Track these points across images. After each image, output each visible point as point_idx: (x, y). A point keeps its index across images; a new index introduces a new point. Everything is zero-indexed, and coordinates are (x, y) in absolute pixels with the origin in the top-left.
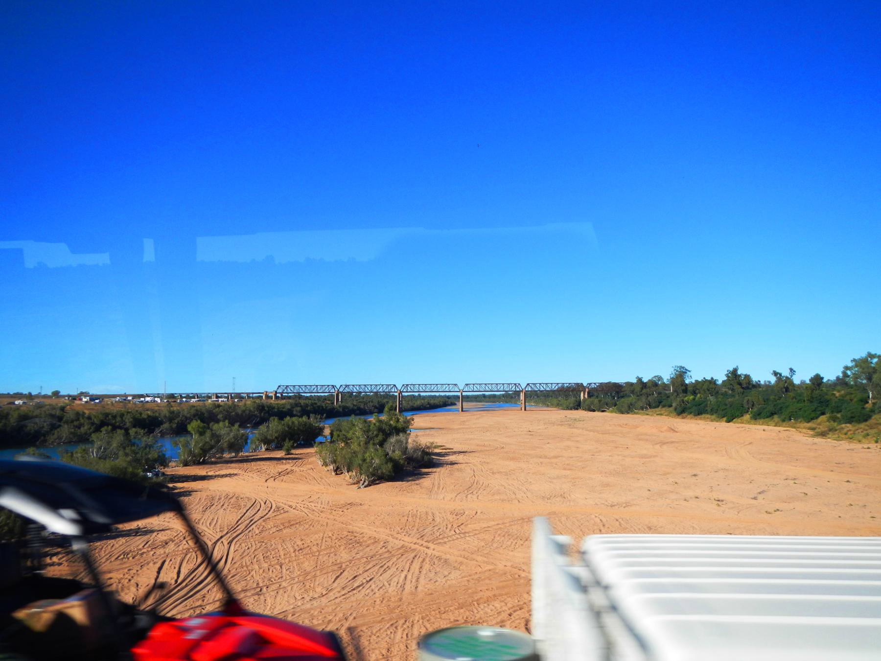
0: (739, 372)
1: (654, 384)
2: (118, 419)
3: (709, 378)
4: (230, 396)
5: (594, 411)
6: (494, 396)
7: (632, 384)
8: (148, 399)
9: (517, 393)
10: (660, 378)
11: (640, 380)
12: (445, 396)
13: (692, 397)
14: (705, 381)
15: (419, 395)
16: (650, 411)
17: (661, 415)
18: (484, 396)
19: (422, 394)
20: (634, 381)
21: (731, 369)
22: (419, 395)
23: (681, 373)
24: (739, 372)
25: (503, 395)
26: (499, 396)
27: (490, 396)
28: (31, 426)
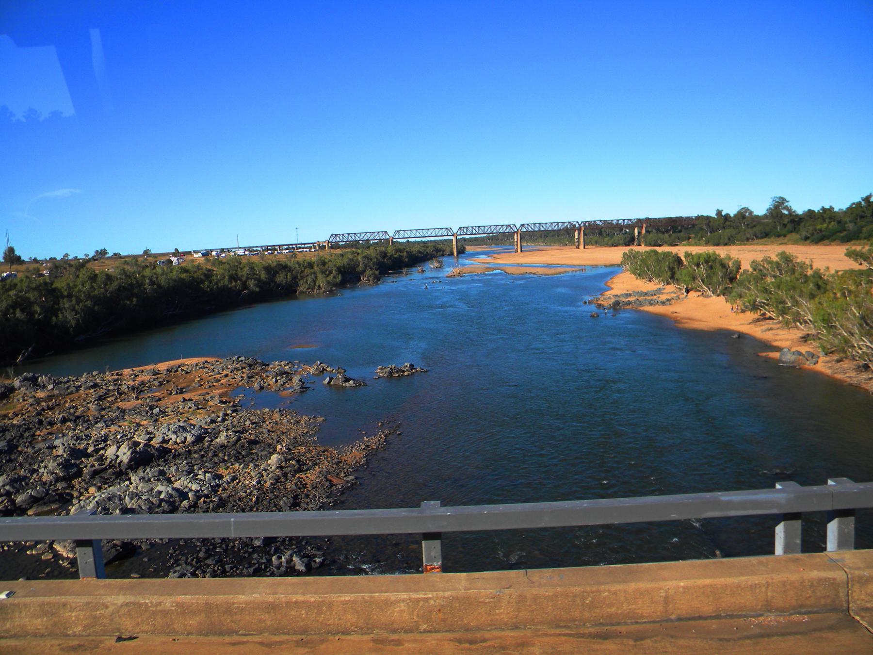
1: (744, 216)
4: (291, 247)
6: (476, 239)
7: (708, 218)
10: (746, 210)
11: (719, 213)
12: (435, 241)
13: (825, 225)
15: (408, 242)
16: (756, 241)
17: (785, 244)
19: (411, 240)
20: (713, 214)
22: (408, 242)
23: (780, 203)
25: (488, 238)
28: (280, 278)
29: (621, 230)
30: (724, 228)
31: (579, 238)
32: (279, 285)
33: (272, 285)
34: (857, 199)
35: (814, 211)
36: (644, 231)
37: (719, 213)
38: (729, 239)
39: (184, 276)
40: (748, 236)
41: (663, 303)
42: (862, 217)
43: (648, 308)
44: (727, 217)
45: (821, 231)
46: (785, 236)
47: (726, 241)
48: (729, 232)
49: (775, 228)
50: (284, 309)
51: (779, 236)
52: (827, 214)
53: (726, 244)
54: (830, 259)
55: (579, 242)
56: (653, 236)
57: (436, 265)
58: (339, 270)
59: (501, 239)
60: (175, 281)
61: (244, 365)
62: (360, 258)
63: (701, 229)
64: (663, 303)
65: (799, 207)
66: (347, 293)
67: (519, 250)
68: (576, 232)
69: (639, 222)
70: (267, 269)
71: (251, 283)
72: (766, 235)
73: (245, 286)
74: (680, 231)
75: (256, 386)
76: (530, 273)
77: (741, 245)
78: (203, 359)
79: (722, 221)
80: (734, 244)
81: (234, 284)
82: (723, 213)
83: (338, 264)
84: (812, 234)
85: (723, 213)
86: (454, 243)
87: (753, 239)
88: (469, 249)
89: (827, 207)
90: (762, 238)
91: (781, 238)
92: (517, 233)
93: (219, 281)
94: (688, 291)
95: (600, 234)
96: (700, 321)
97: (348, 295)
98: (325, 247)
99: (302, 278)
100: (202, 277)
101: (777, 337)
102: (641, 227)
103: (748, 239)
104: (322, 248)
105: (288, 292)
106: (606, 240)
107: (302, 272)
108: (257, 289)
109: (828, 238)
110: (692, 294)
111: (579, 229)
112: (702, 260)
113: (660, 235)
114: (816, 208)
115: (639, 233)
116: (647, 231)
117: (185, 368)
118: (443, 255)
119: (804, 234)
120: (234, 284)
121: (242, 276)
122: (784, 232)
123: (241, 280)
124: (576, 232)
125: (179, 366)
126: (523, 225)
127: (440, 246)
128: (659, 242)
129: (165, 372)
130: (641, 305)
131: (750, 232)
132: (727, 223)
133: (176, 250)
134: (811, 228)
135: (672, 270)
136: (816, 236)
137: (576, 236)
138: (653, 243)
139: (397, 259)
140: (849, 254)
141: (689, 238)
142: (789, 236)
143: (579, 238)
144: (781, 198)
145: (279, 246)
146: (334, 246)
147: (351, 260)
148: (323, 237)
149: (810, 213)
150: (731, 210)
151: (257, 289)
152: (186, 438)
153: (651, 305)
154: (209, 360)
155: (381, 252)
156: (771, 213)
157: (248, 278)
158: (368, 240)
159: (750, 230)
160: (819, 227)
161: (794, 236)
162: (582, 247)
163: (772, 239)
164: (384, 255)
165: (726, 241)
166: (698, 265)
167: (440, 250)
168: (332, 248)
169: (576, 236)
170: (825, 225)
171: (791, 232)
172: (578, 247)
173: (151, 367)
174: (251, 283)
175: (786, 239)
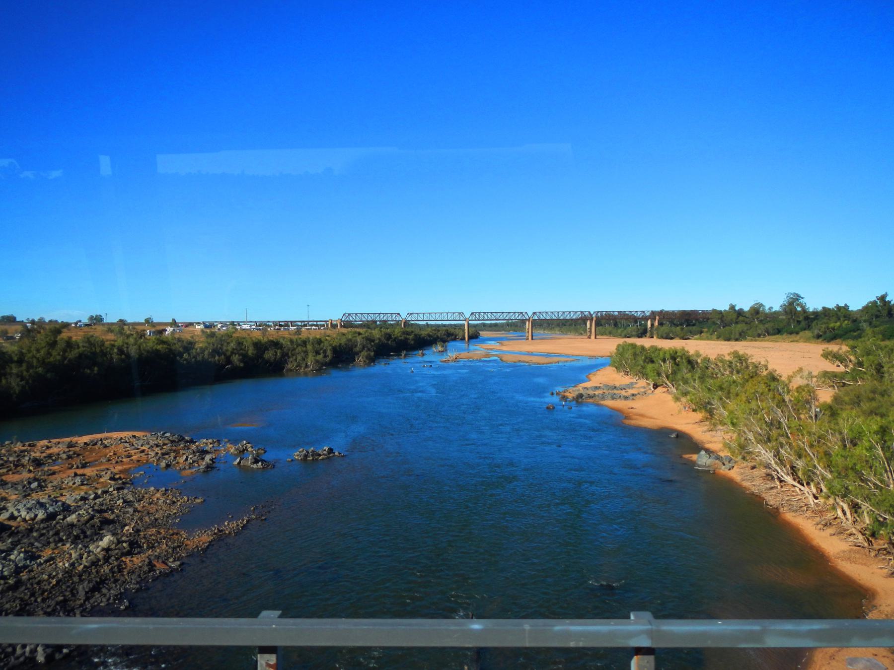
0: (887, 299)
1: (756, 311)
2: (317, 346)
3: (843, 305)
5: (672, 338)
6: (496, 325)
7: (720, 312)
8: (245, 327)
9: (523, 322)
10: (762, 305)
11: (732, 307)
13: (838, 324)
14: (839, 308)
15: (427, 324)
16: (768, 337)
18: (484, 325)
19: (430, 323)
20: (724, 307)
21: (879, 295)
24: (887, 299)
25: (508, 324)
26: (502, 325)
27: (491, 325)
28: (269, 355)
29: (636, 322)
30: (737, 323)
31: (590, 328)
32: (268, 361)
33: (260, 361)
34: (874, 299)
35: (829, 309)
36: (656, 324)
37: (732, 307)
38: (740, 334)
39: (159, 347)
40: (760, 332)
41: (626, 398)
43: (609, 403)
44: (740, 313)
45: (833, 329)
46: (797, 333)
47: (737, 336)
48: (740, 327)
49: (789, 324)
50: (270, 386)
51: (791, 333)
52: (842, 312)
53: (737, 340)
54: (795, 361)
55: (590, 331)
57: (440, 348)
58: (334, 350)
59: (515, 326)
60: (148, 352)
61: (167, 442)
62: (359, 339)
63: (714, 323)
64: (626, 398)
65: (814, 303)
66: (334, 373)
67: (530, 338)
68: (588, 322)
69: (653, 314)
70: (257, 345)
71: (235, 359)
72: (779, 332)
73: (228, 360)
74: (694, 325)
75: (163, 464)
76: (524, 362)
77: (752, 340)
78: (131, 433)
79: (735, 316)
80: (745, 339)
81: (217, 358)
82: (737, 308)
83: (334, 344)
84: (825, 333)
85: (737, 308)
86: (466, 328)
87: (764, 335)
88: (484, 334)
90: (774, 334)
91: (793, 336)
92: (529, 320)
93: (198, 354)
94: (656, 386)
95: (616, 325)
96: (651, 418)
97: (337, 376)
98: (337, 325)
99: (293, 355)
100: (181, 349)
101: (714, 439)
102: (654, 319)
103: (759, 336)
104: (334, 326)
105: (276, 369)
106: (619, 331)
107: (294, 349)
108: (242, 365)
109: (840, 337)
110: (660, 389)
112: (667, 356)
113: (673, 328)
114: (831, 305)
115: (652, 325)
116: (661, 324)
117: (106, 442)
118: (455, 339)
119: (816, 332)
120: (217, 358)
121: (227, 350)
122: (797, 329)
123: (225, 355)
124: (588, 322)
125: (101, 440)
126: (535, 313)
127: (452, 331)
128: (671, 335)
129: (82, 445)
130: (603, 398)
131: (762, 328)
132: (741, 318)
133: (174, 320)
134: (824, 326)
135: (641, 363)
136: (828, 334)
137: (588, 326)
138: (665, 336)
139: (400, 341)
140: (826, 355)
141: (701, 332)
142: (801, 333)
143: (590, 328)
144: (795, 294)
145: (291, 322)
146: (347, 324)
147: (350, 340)
148: (336, 315)
149: (826, 312)
150: (745, 305)
151: (242, 365)
152: (36, 516)
153: (613, 398)
154: (137, 434)
155: (386, 334)
156: (785, 310)
157: (232, 353)
158: (385, 321)
159: (761, 326)
160: (832, 325)
161: (808, 333)
162: (593, 337)
163: (784, 336)
164: (389, 336)
165: (737, 336)
166: (664, 361)
167: (452, 335)
168: (344, 327)
169: (588, 326)
170: (838, 324)
171: (805, 329)
172: (589, 337)
173: (69, 439)
174: (235, 359)
175: (798, 337)
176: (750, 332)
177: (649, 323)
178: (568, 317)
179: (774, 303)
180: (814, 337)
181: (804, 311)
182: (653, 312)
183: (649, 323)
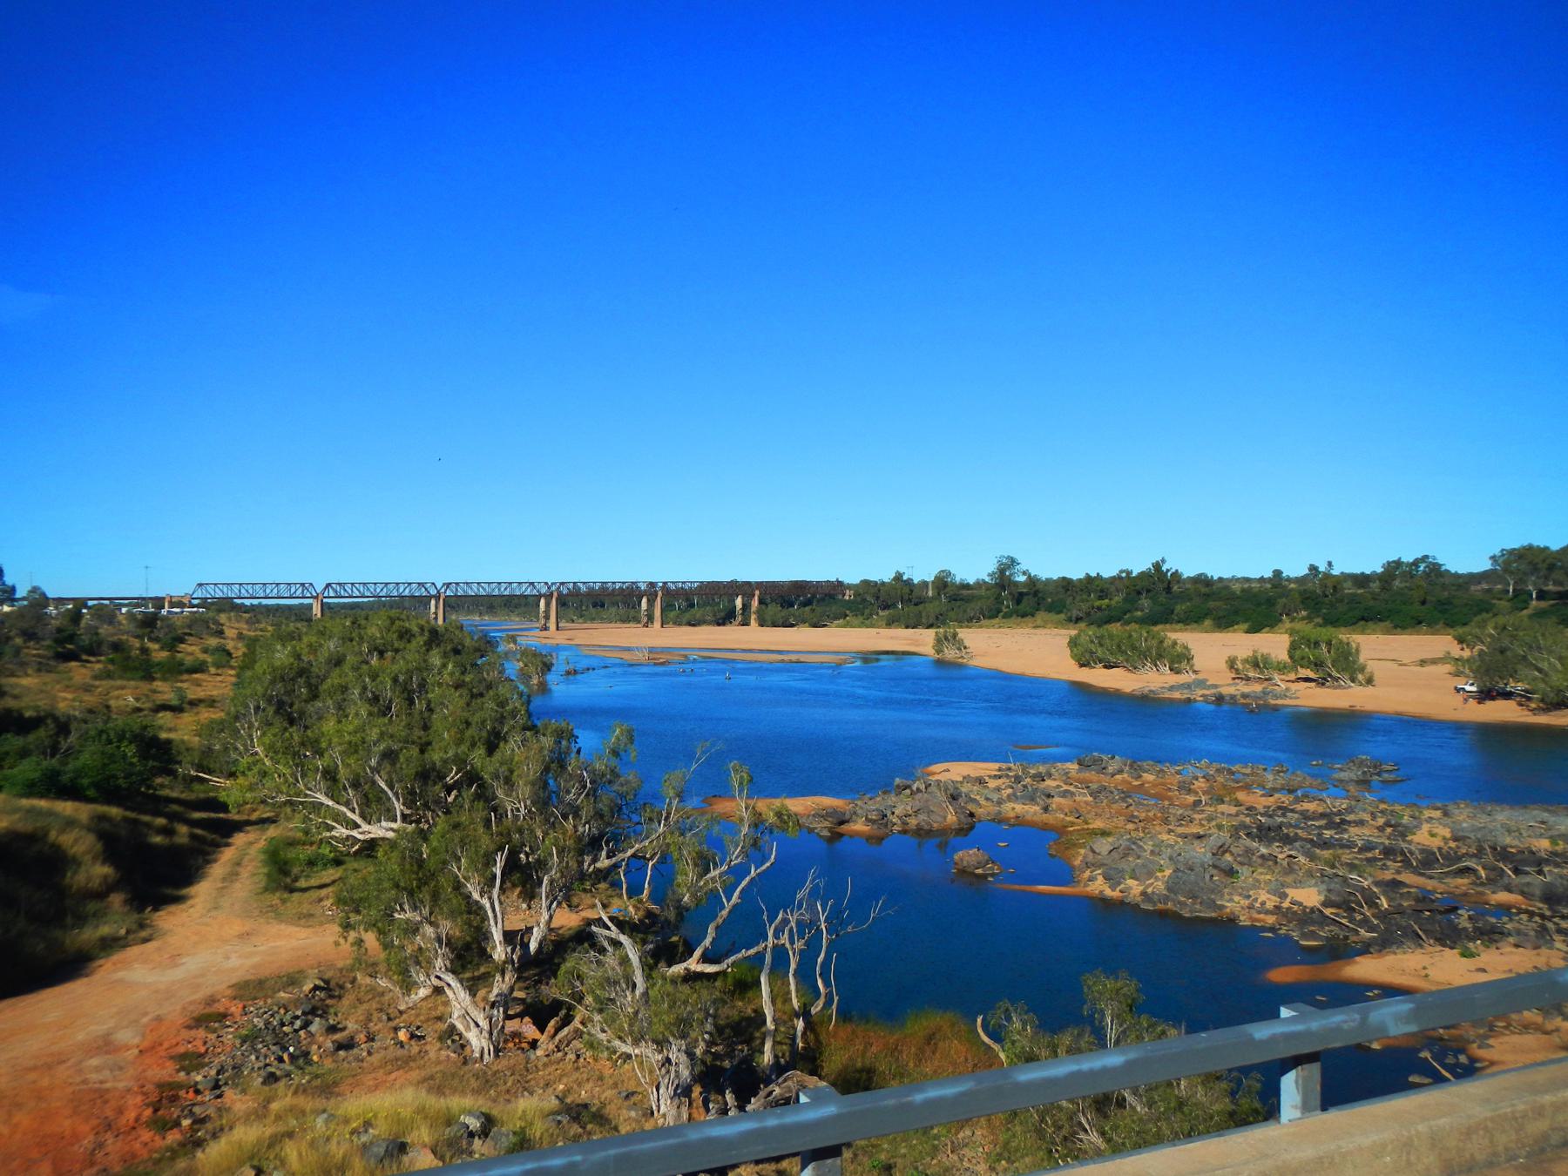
5: (792, 626)
16: (984, 622)
36: (755, 603)
42: (1148, 591)
45: (1099, 608)
56: (773, 610)
67: (552, 624)
68: (644, 600)
79: (906, 590)
84: (1088, 614)
89: (1093, 574)
90: (991, 617)
103: (970, 620)
111: (549, 597)
114: (1076, 574)
115: (746, 607)
116: (761, 602)
119: (1075, 613)
149: (1066, 584)
162: (657, 624)
176: (951, 614)
177: (739, 602)
178: (496, 592)
179: (974, 569)
180: (1070, 620)
181: (1033, 581)
182: (652, 585)
183: (739, 602)
